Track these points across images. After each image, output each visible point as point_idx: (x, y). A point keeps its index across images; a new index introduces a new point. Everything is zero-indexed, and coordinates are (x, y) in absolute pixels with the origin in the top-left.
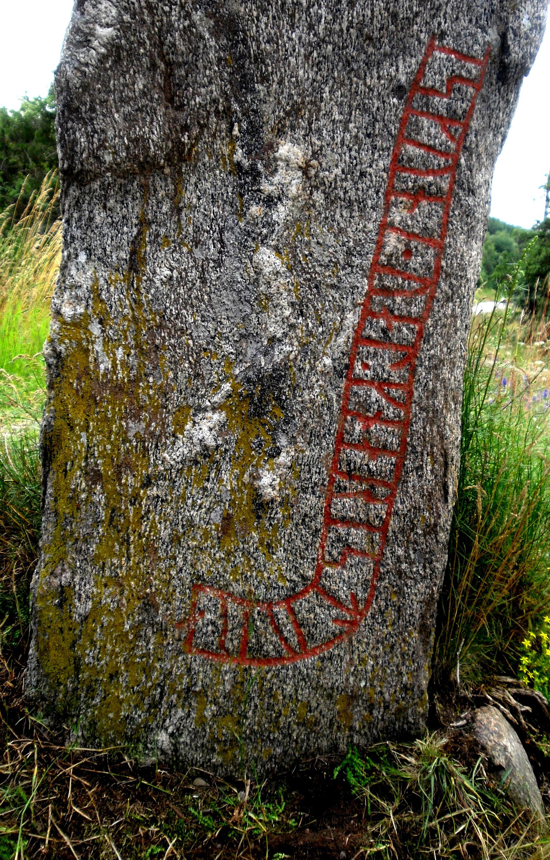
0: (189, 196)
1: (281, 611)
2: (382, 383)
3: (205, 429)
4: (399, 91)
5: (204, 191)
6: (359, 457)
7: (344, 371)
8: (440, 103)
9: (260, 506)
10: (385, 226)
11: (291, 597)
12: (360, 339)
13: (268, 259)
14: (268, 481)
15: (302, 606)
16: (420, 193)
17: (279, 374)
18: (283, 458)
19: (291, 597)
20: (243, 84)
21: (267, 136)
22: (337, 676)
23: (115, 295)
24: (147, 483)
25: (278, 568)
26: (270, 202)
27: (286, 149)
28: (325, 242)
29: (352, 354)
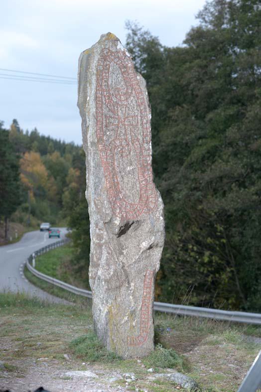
0: (121, 290)
1: (137, 339)
2: (145, 310)
3: (126, 318)
4: (145, 276)
5: (123, 289)
6: (144, 320)
7: (141, 309)
8: (149, 277)
9: (134, 327)
10: (144, 292)
11: (138, 337)
12: (142, 306)
13: (131, 297)
14: (134, 324)
15: (139, 338)
16: (147, 288)
17: (134, 310)
18: (135, 321)
19: (138, 337)
20: (127, 277)
21: (130, 282)
22: (145, 346)
23: (114, 303)
24: (121, 325)
25: (137, 333)
26: (131, 290)
27: (132, 284)
28: (137, 294)
29: (141, 307)
